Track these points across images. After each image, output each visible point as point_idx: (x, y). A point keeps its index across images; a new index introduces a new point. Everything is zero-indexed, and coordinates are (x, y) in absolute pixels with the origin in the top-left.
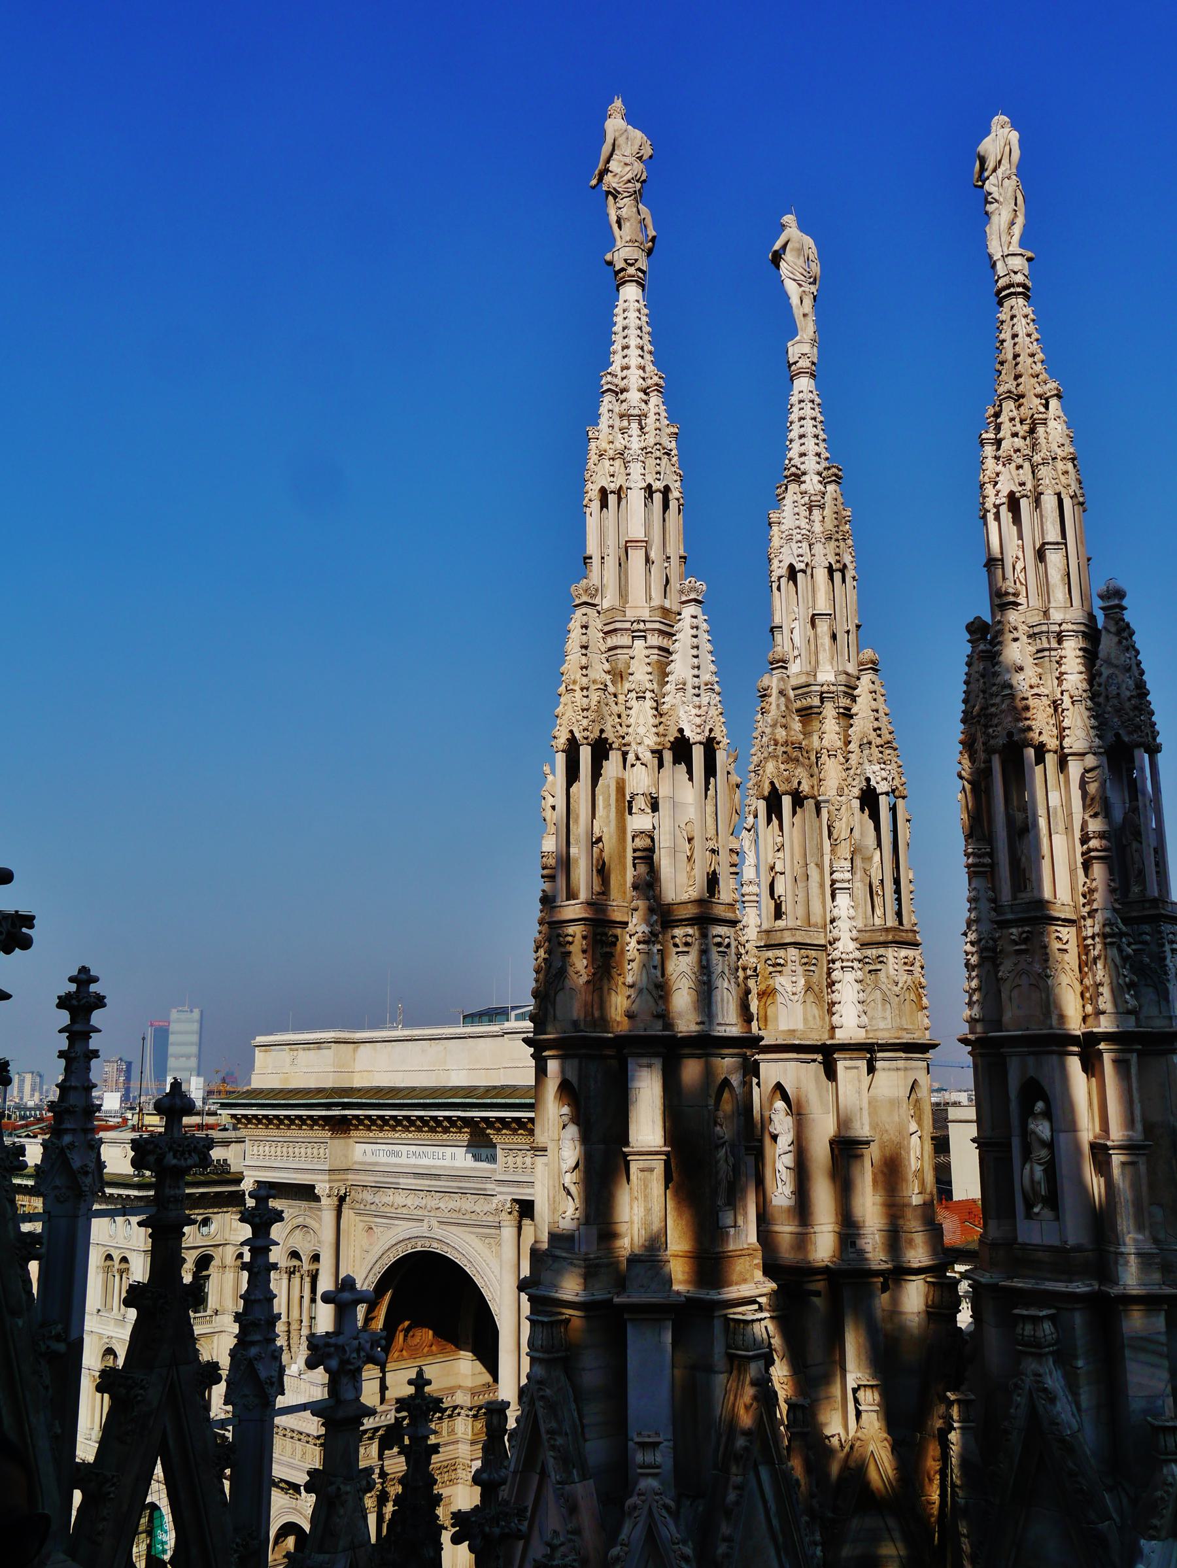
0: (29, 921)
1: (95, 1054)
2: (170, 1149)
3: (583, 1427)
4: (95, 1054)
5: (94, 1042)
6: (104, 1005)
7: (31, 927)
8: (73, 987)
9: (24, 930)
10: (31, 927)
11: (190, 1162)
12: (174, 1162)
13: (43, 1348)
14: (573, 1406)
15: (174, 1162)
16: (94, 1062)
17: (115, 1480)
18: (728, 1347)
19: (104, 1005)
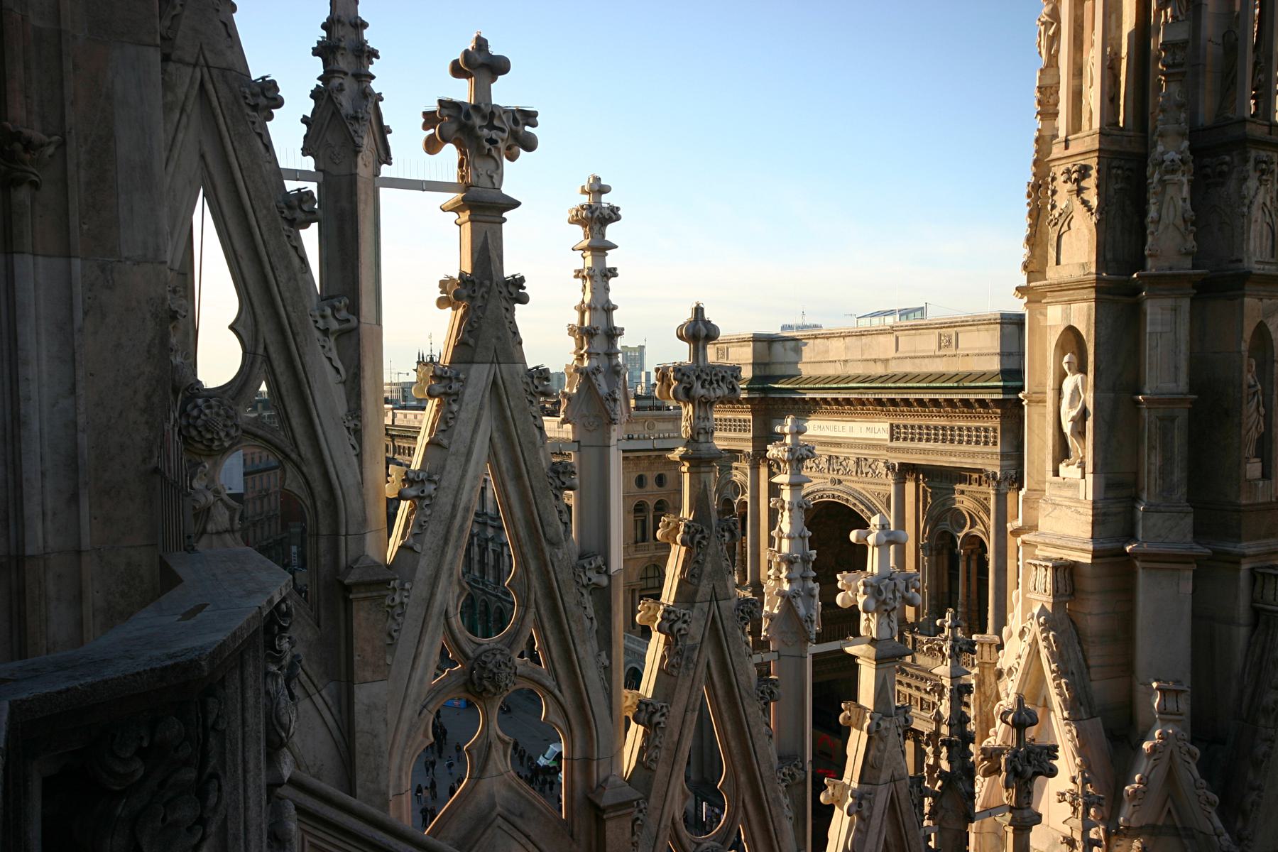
0: (529, 117)
1: (613, 272)
2: (698, 377)
3: (1088, 667)
4: (613, 272)
5: (611, 260)
6: (618, 218)
7: (534, 125)
8: (585, 200)
9: (527, 128)
10: (534, 125)
11: (719, 393)
12: (702, 392)
13: (585, 581)
14: (1078, 648)
15: (702, 392)
16: (612, 281)
17: (665, 710)
18: (1253, 600)
19: (618, 218)
